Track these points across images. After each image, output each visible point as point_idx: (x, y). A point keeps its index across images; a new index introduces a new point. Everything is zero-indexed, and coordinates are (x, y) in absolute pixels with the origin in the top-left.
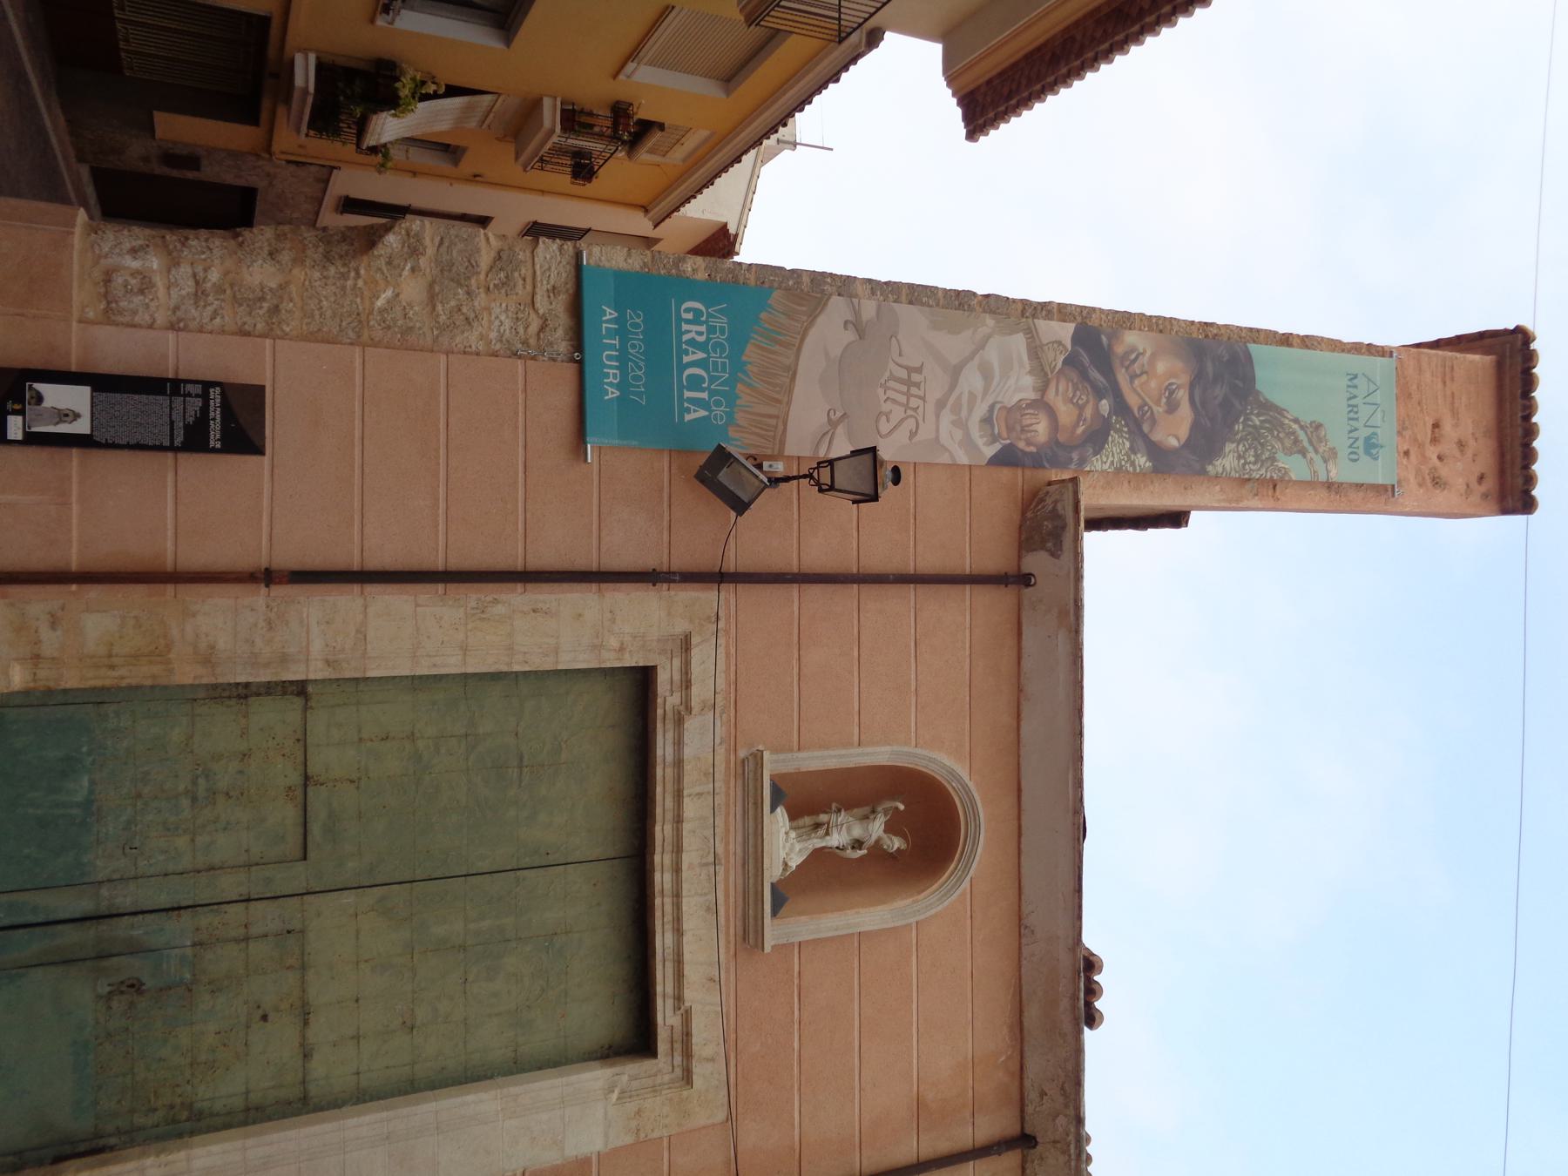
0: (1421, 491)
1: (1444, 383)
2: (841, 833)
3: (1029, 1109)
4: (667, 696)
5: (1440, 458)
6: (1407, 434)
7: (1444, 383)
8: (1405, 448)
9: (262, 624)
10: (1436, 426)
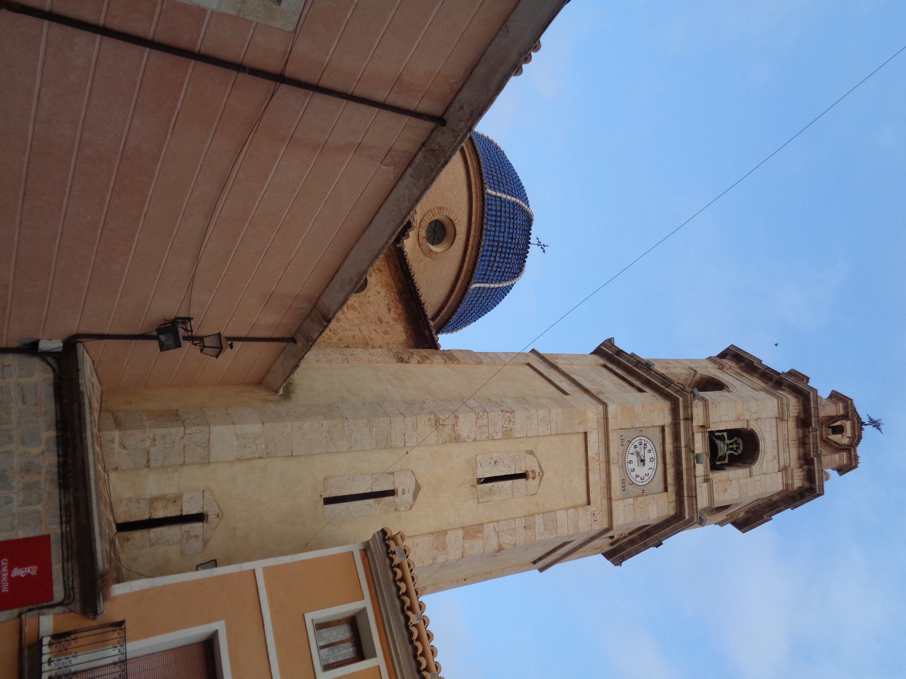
3: (451, 110)
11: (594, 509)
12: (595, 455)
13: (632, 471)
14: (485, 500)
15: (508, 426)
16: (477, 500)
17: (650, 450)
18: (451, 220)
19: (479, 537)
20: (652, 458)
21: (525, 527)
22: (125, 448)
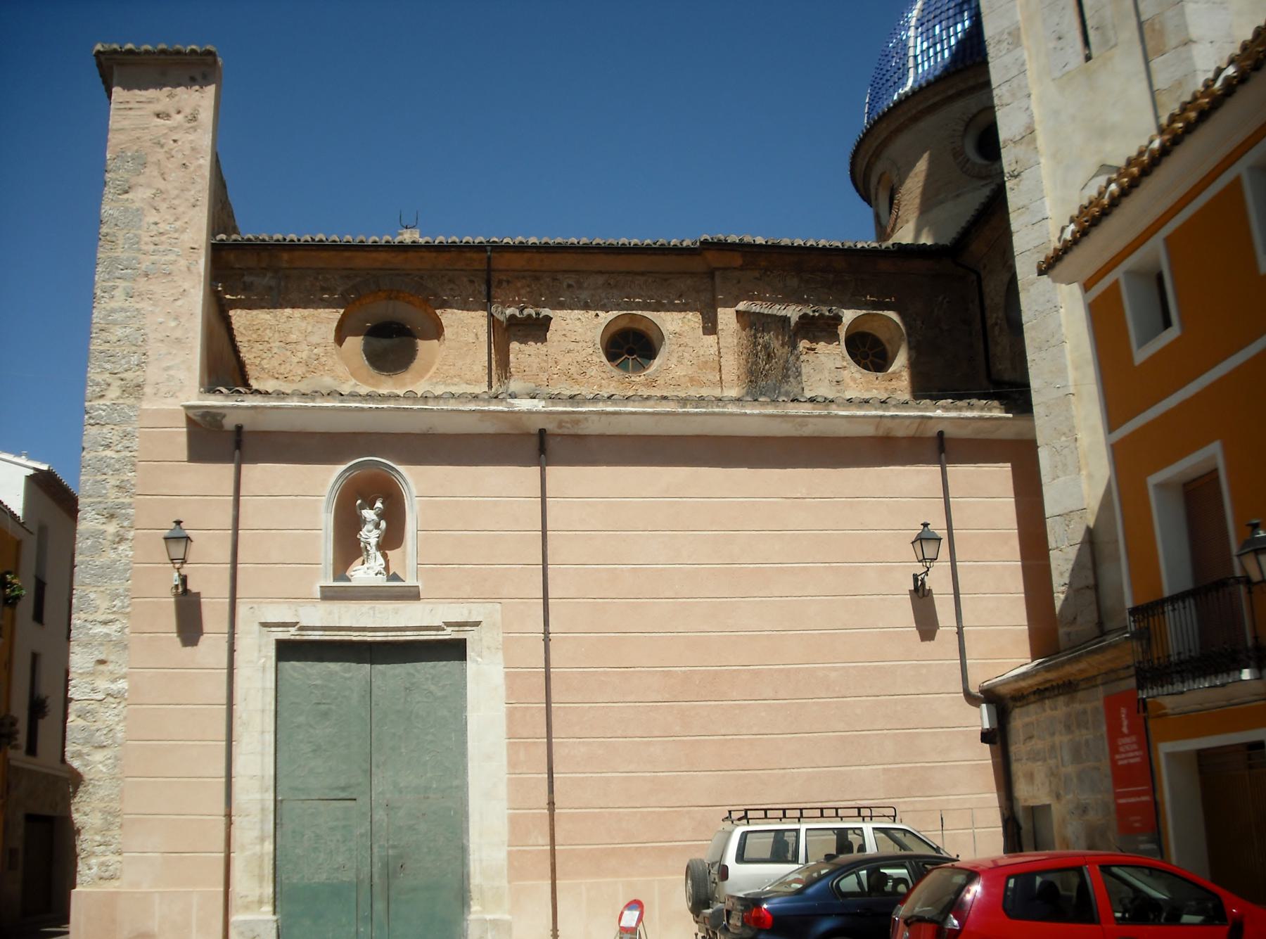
0: (199, 130)
1: (130, 109)
2: (370, 535)
4: (290, 634)
5: (179, 112)
6: (163, 141)
7: (130, 109)
8: (172, 142)
9: (247, 818)
10: (158, 116)
15: (1005, 44)
22: (1075, 618)
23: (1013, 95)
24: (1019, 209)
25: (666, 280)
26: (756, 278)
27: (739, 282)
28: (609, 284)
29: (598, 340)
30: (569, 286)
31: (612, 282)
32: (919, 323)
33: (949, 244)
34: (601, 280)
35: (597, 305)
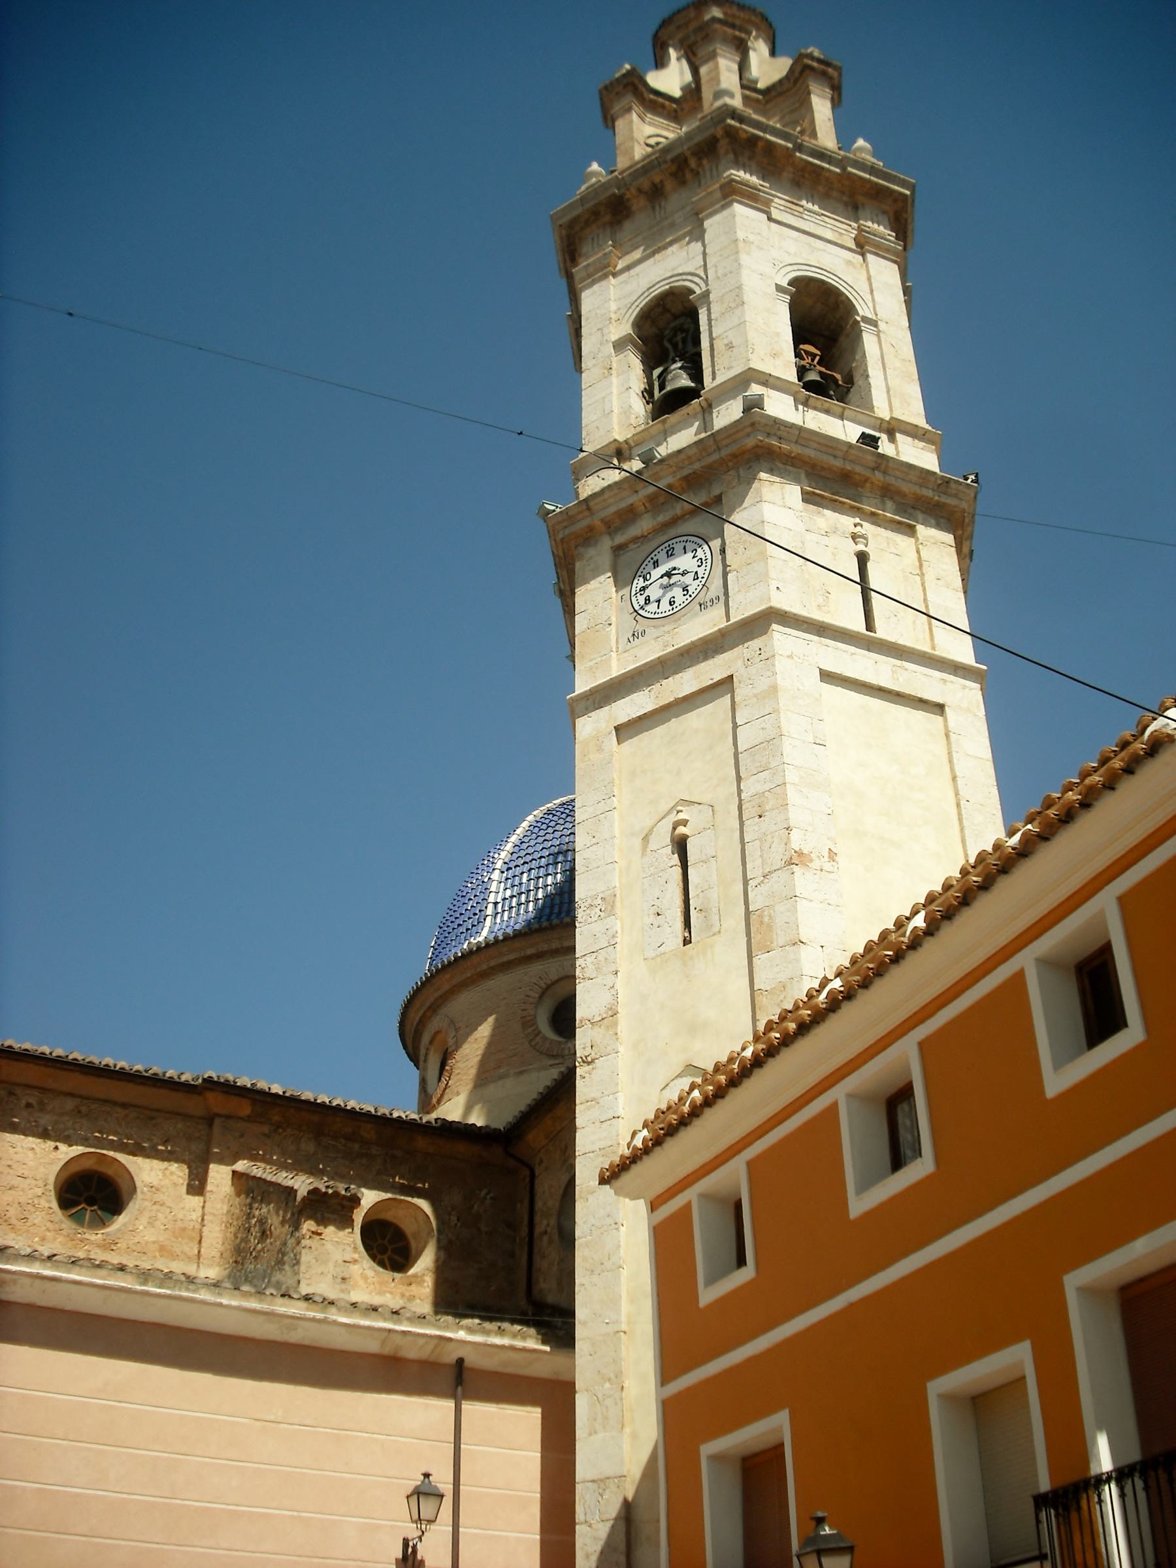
11: (740, 663)
12: (652, 693)
13: (687, 590)
14: (717, 917)
16: (714, 937)
17: (654, 563)
18: (541, 997)
19: (770, 917)
20: (667, 552)
21: (760, 816)
23: (598, 969)
24: (587, 1102)
25: (152, 1118)
26: (265, 1135)
27: (242, 1136)
28: (79, 1112)
29: (51, 1180)
30: (29, 1105)
31: (84, 1109)
32: (454, 1218)
33: (502, 1129)
34: (70, 1104)
35: (60, 1135)
